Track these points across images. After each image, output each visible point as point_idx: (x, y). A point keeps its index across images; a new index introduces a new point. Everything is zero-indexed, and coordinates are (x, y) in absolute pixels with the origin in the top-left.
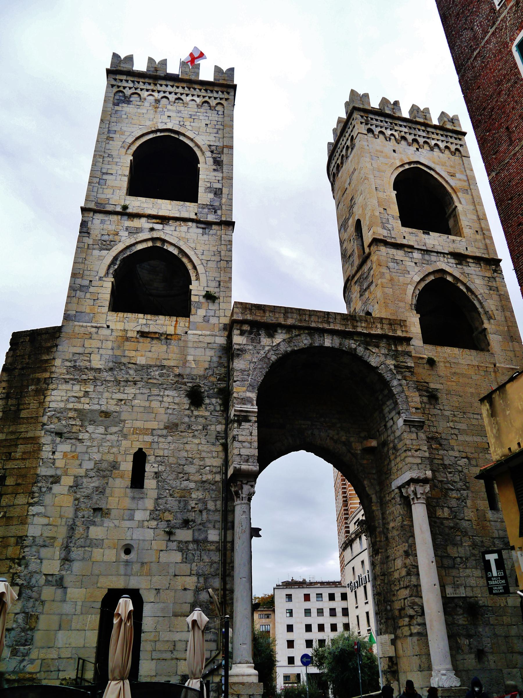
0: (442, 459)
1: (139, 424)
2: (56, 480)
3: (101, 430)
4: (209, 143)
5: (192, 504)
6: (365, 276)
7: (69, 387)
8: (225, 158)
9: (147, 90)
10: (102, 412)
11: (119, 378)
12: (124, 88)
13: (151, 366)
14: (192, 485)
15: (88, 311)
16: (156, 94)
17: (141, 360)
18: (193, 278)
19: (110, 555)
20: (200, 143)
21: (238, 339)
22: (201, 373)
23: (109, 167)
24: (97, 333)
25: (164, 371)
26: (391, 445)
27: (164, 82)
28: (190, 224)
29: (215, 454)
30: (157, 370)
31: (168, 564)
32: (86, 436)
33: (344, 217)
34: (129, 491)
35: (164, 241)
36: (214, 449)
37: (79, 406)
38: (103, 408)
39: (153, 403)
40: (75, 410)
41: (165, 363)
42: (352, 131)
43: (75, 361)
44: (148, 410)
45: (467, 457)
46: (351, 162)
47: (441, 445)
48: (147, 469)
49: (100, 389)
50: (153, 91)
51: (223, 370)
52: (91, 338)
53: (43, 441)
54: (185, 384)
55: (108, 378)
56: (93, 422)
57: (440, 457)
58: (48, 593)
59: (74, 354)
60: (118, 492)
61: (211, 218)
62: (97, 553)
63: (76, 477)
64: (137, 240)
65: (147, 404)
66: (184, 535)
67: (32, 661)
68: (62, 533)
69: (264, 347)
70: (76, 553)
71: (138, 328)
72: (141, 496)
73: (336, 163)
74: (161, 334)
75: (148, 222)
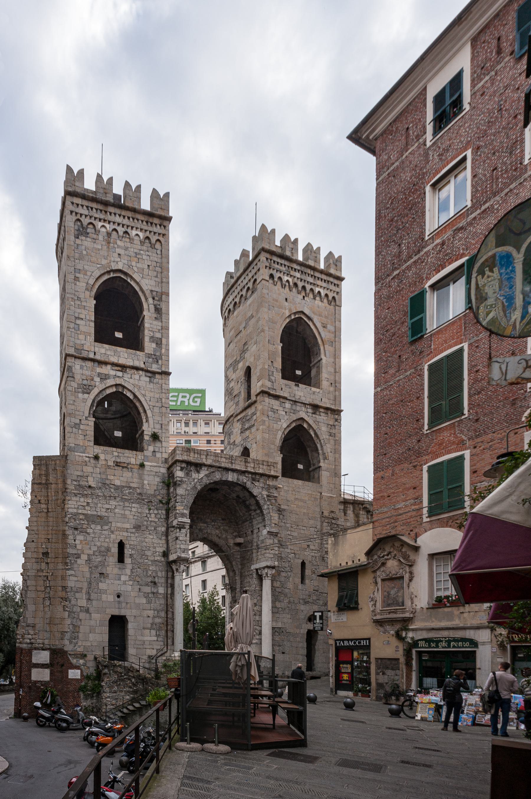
1: (119, 525)
2: (78, 556)
3: (99, 527)
4: (150, 288)
5: (150, 573)
7: (77, 499)
8: (163, 306)
10: (98, 516)
11: (106, 494)
13: (123, 487)
15: (81, 444)
17: (118, 483)
19: (111, 598)
20: (145, 288)
22: (153, 493)
24: (89, 461)
28: (141, 372)
29: (161, 545)
31: (139, 604)
32: (91, 531)
35: (124, 387)
37: (85, 512)
38: (99, 514)
40: (83, 514)
41: (132, 485)
43: (79, 481)
44: (124, 516)
49: (95, 501)
52: (86, 465)
53: (67, 533)
54: (143, 500)
55: (99, 494)
56: (94, 522)
58: (82, 615)
59: (78, 476)
62: (104, 597)
63: (88, 555)
64: (107, 386)
65: (123, 512)
66: (147, 589)
67: (79, 647)
68: (85, 585)
69: (194, 479)
70: (93, 596)
71: (114, 459)
74: (128, 464)
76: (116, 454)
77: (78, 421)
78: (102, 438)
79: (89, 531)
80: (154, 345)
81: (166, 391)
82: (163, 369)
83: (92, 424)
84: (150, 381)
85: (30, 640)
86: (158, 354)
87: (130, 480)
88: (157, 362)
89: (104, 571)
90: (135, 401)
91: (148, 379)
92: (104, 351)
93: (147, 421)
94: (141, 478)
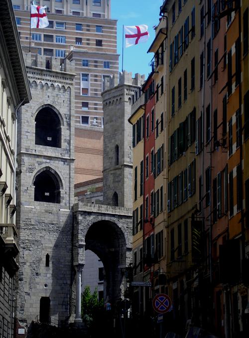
1: (46, 245)
2: (25, 263)
6: (117, 175)
14: (63, 266)
16: (43, 82)
18: (61, 185)
20: (61, 113)
21: (80, 218)
23: (27, 128)
26: (120, 254)
27: (45, 73)
33: (109, 134)
35: (50, 168)
36: (68, 254)
41: (54, 222)
44: (49, 240)
46: (118, 109)
51: (71, 225)
55: (37, 228)
58: (27, 297)
61: (67, 157)
66: (61, 282)
76: (45, 205)
77: (26, 188)
78: (39, 197)
79: (31, 249)
83: (34, 189)
89: (38, 272)
93: (62, 186)
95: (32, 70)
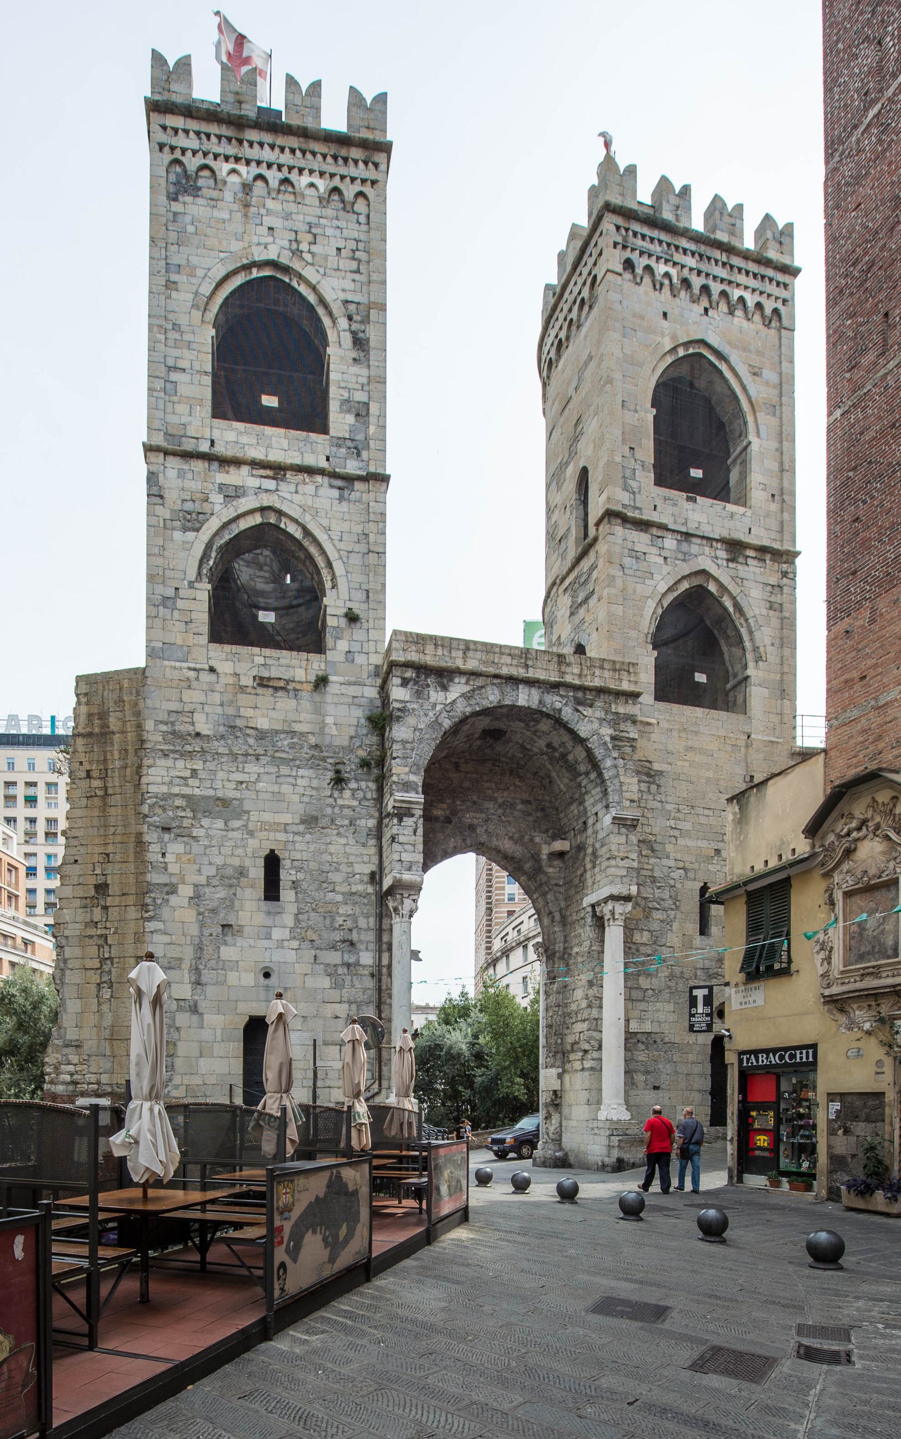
0: (652, 870)
1: (267, 817)
9: (227, 159)
12: (184, 151)
25: (295, 740)
30: (285, 739)
34: (263, 904)
35: (280, 513)
39: (283, 787)
41: (297, 727)
42: (595, 264)
44: (278, 797)
45: (684, 868)
47: (653, 851)
48: (282, 877)
50: (237, 160)
54: (324, 759)
57: (650, 867)
60: (249, 905)
62: (232, 978)
72: (278, 910)
73: (557, 336)
74: (288, 682)
75: (253, 476)
80: (350, 419)
81: (379, 518)
82: (372, 469)
84: (341, 499)
85: (72, 1075)
86: (360, 437)
87: (292, 716)
88: (359, 454)
90: (306, 543)
91: (336, 493)
92: (234, 436)
94: (318, 710)
95: (193, 125)
